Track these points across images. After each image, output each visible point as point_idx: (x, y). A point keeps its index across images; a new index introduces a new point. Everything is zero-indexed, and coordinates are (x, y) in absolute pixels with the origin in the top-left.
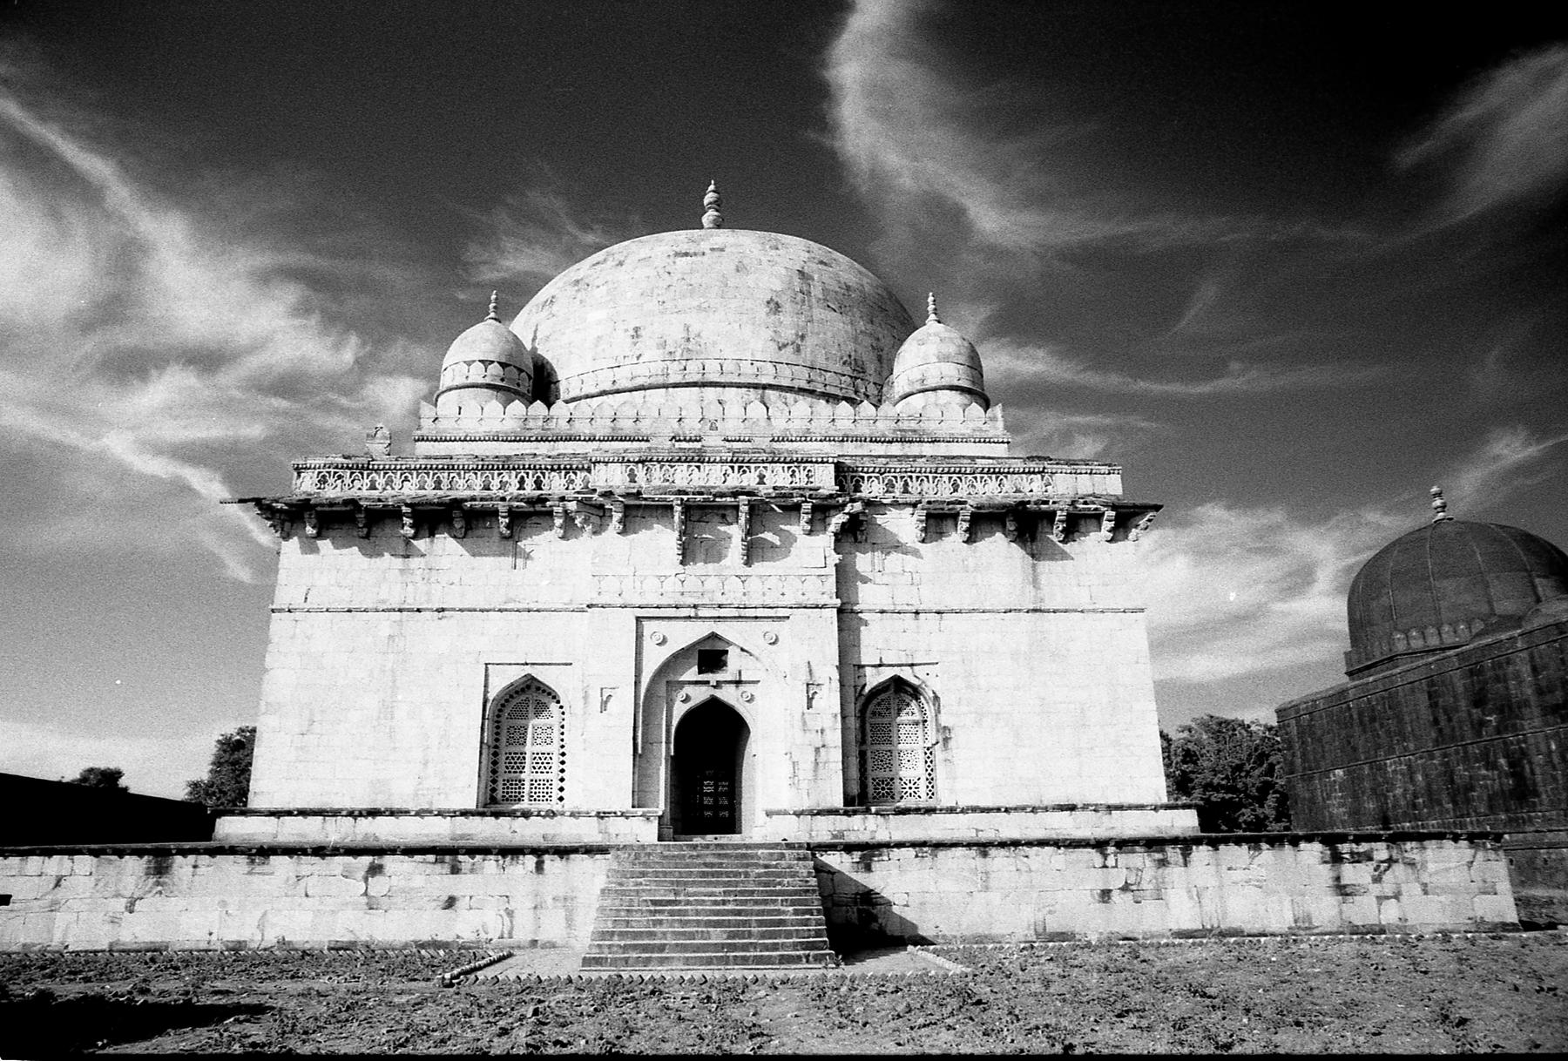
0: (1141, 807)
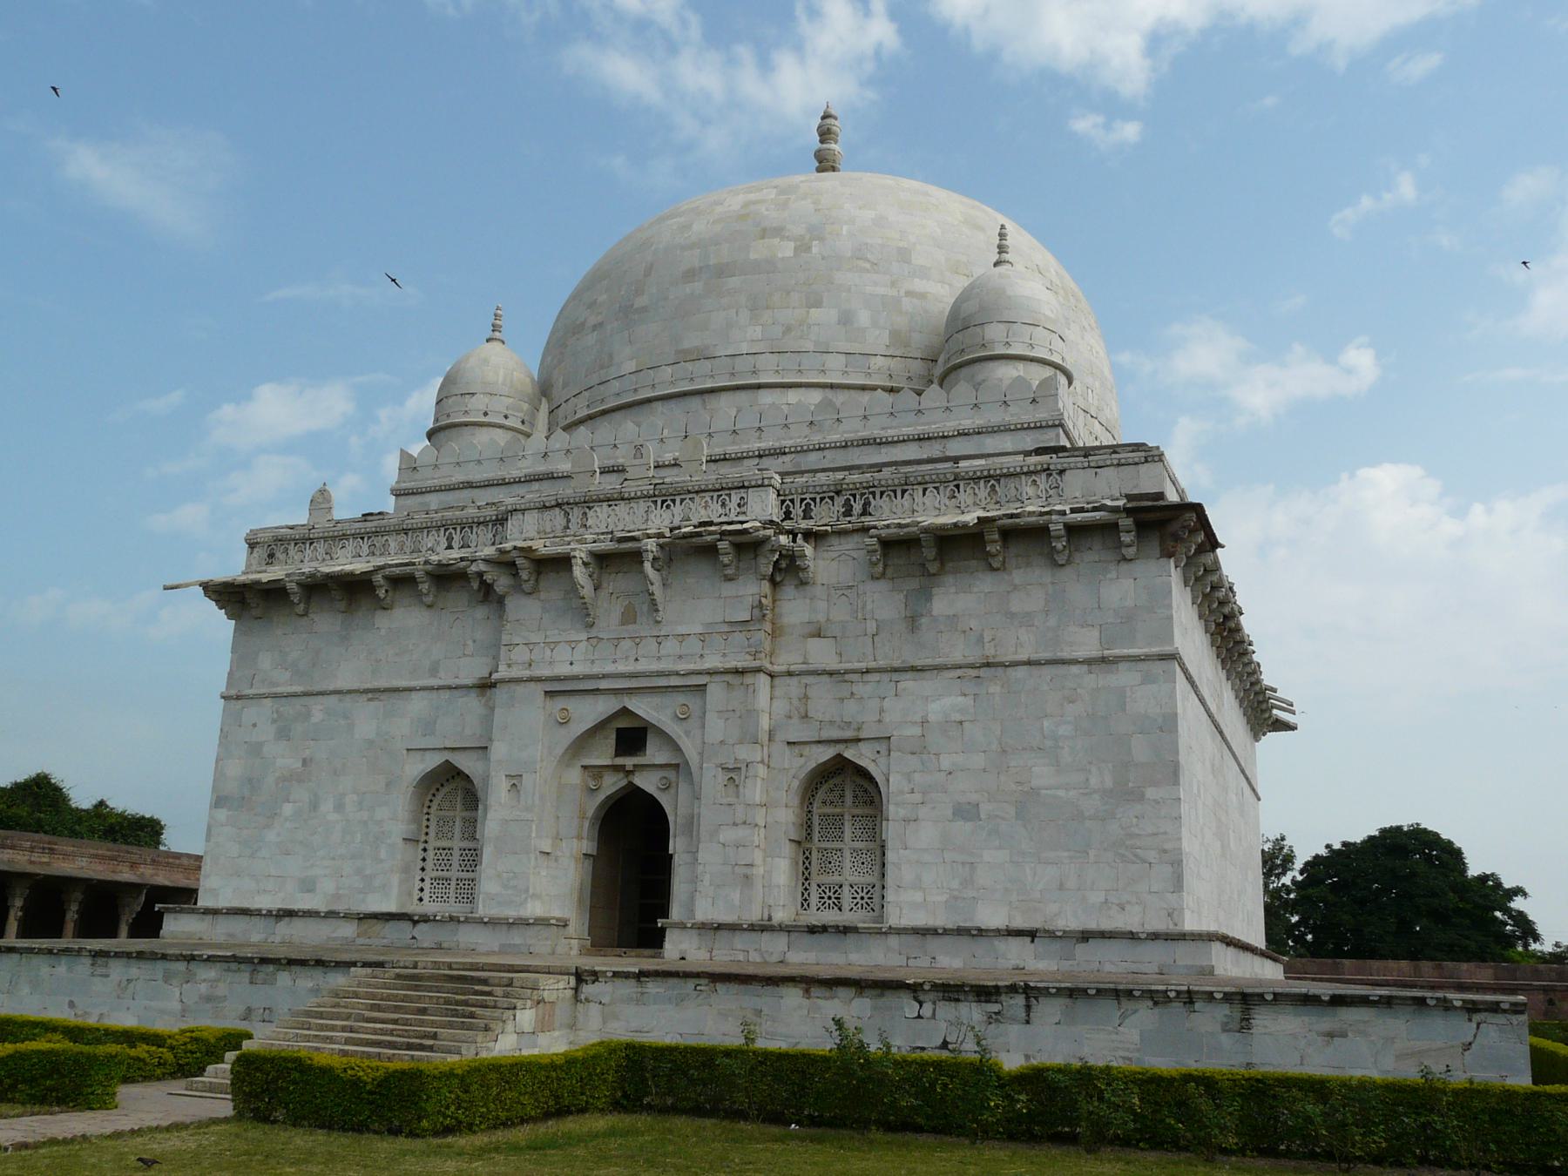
0: (1132, 936)
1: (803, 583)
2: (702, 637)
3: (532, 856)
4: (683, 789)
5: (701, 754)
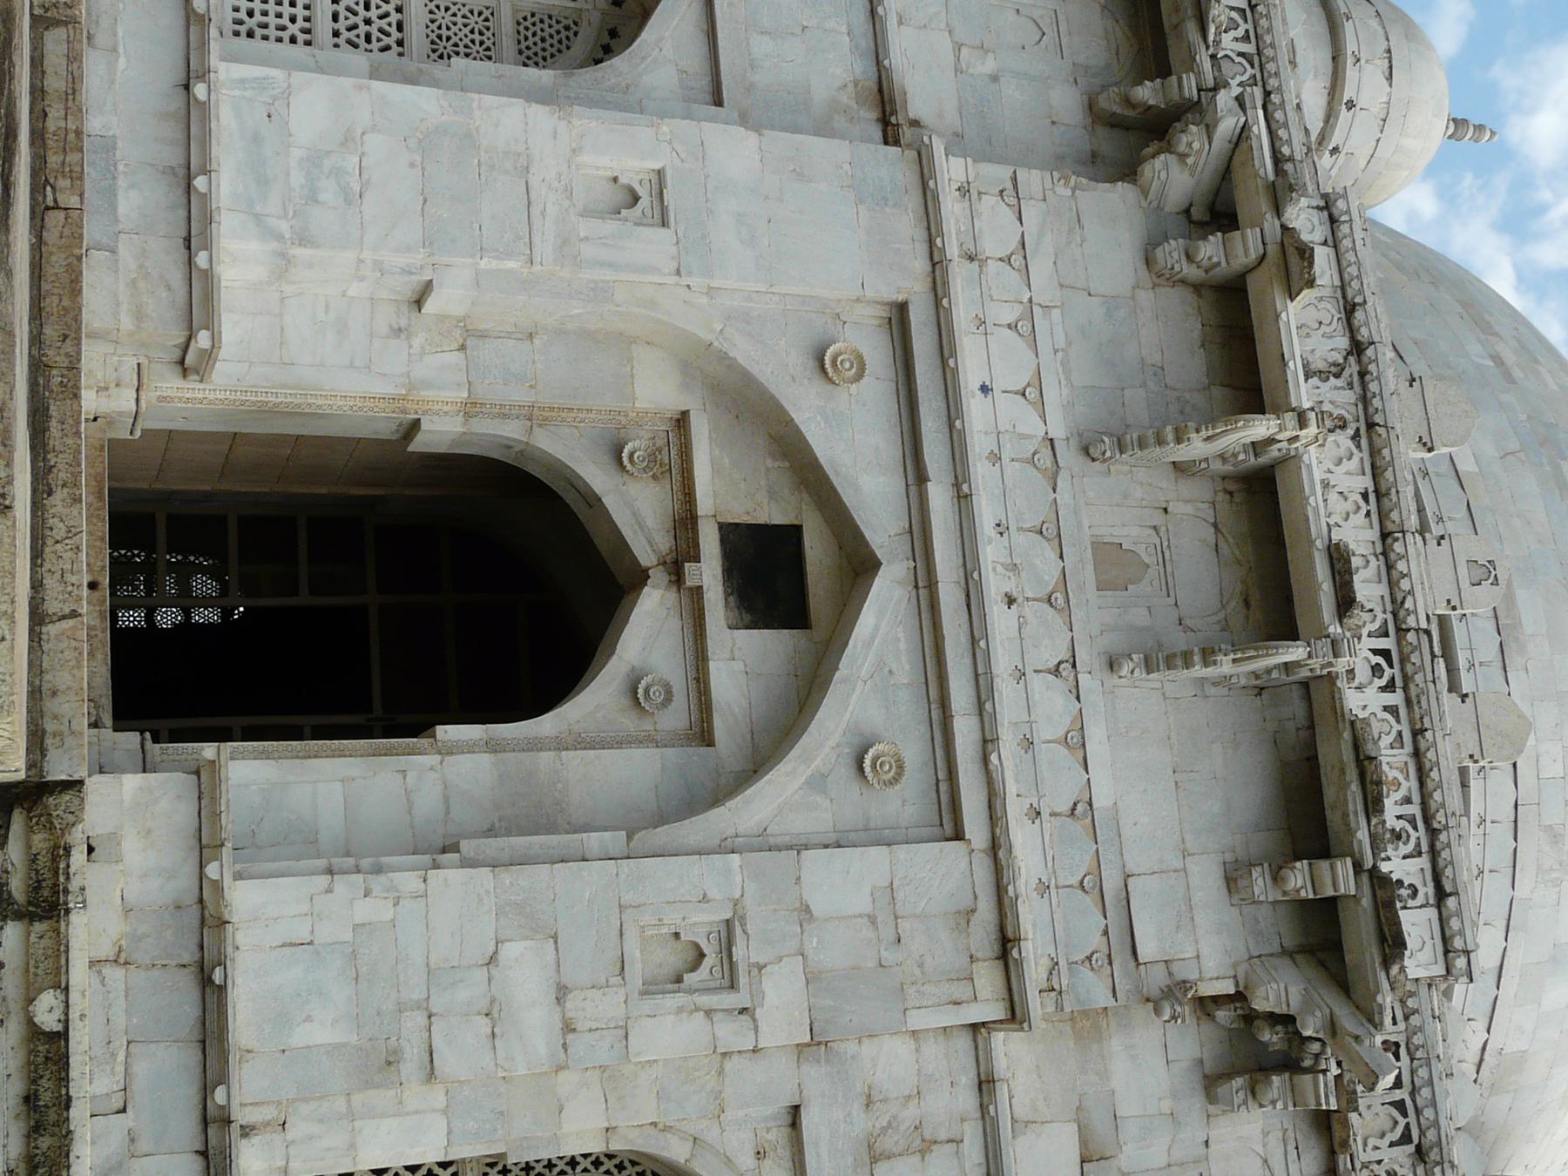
1: (1211, 1083)
2: (1082, 809)
3: (418, 258)
4: (634, 771)
5: (763, 843)
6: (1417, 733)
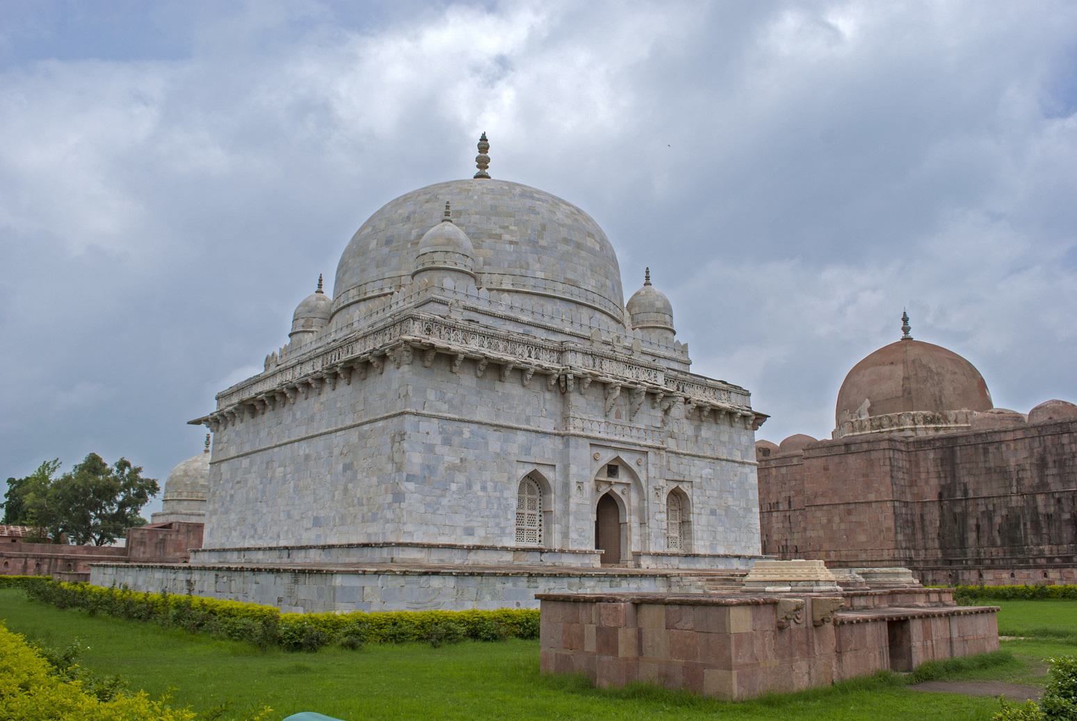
6: (639, 365)
